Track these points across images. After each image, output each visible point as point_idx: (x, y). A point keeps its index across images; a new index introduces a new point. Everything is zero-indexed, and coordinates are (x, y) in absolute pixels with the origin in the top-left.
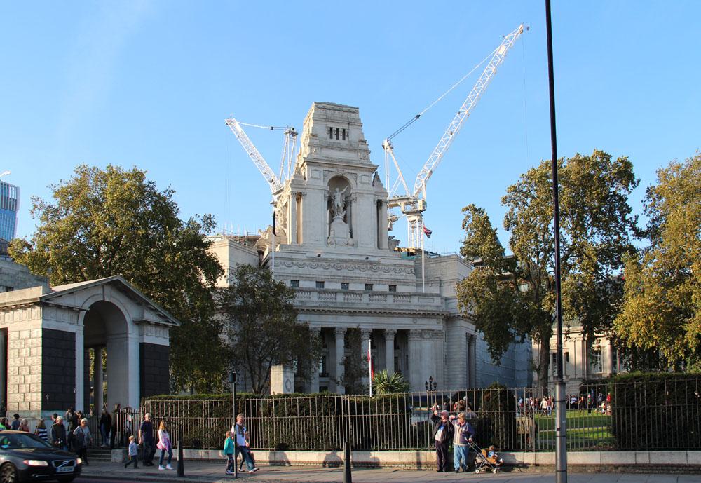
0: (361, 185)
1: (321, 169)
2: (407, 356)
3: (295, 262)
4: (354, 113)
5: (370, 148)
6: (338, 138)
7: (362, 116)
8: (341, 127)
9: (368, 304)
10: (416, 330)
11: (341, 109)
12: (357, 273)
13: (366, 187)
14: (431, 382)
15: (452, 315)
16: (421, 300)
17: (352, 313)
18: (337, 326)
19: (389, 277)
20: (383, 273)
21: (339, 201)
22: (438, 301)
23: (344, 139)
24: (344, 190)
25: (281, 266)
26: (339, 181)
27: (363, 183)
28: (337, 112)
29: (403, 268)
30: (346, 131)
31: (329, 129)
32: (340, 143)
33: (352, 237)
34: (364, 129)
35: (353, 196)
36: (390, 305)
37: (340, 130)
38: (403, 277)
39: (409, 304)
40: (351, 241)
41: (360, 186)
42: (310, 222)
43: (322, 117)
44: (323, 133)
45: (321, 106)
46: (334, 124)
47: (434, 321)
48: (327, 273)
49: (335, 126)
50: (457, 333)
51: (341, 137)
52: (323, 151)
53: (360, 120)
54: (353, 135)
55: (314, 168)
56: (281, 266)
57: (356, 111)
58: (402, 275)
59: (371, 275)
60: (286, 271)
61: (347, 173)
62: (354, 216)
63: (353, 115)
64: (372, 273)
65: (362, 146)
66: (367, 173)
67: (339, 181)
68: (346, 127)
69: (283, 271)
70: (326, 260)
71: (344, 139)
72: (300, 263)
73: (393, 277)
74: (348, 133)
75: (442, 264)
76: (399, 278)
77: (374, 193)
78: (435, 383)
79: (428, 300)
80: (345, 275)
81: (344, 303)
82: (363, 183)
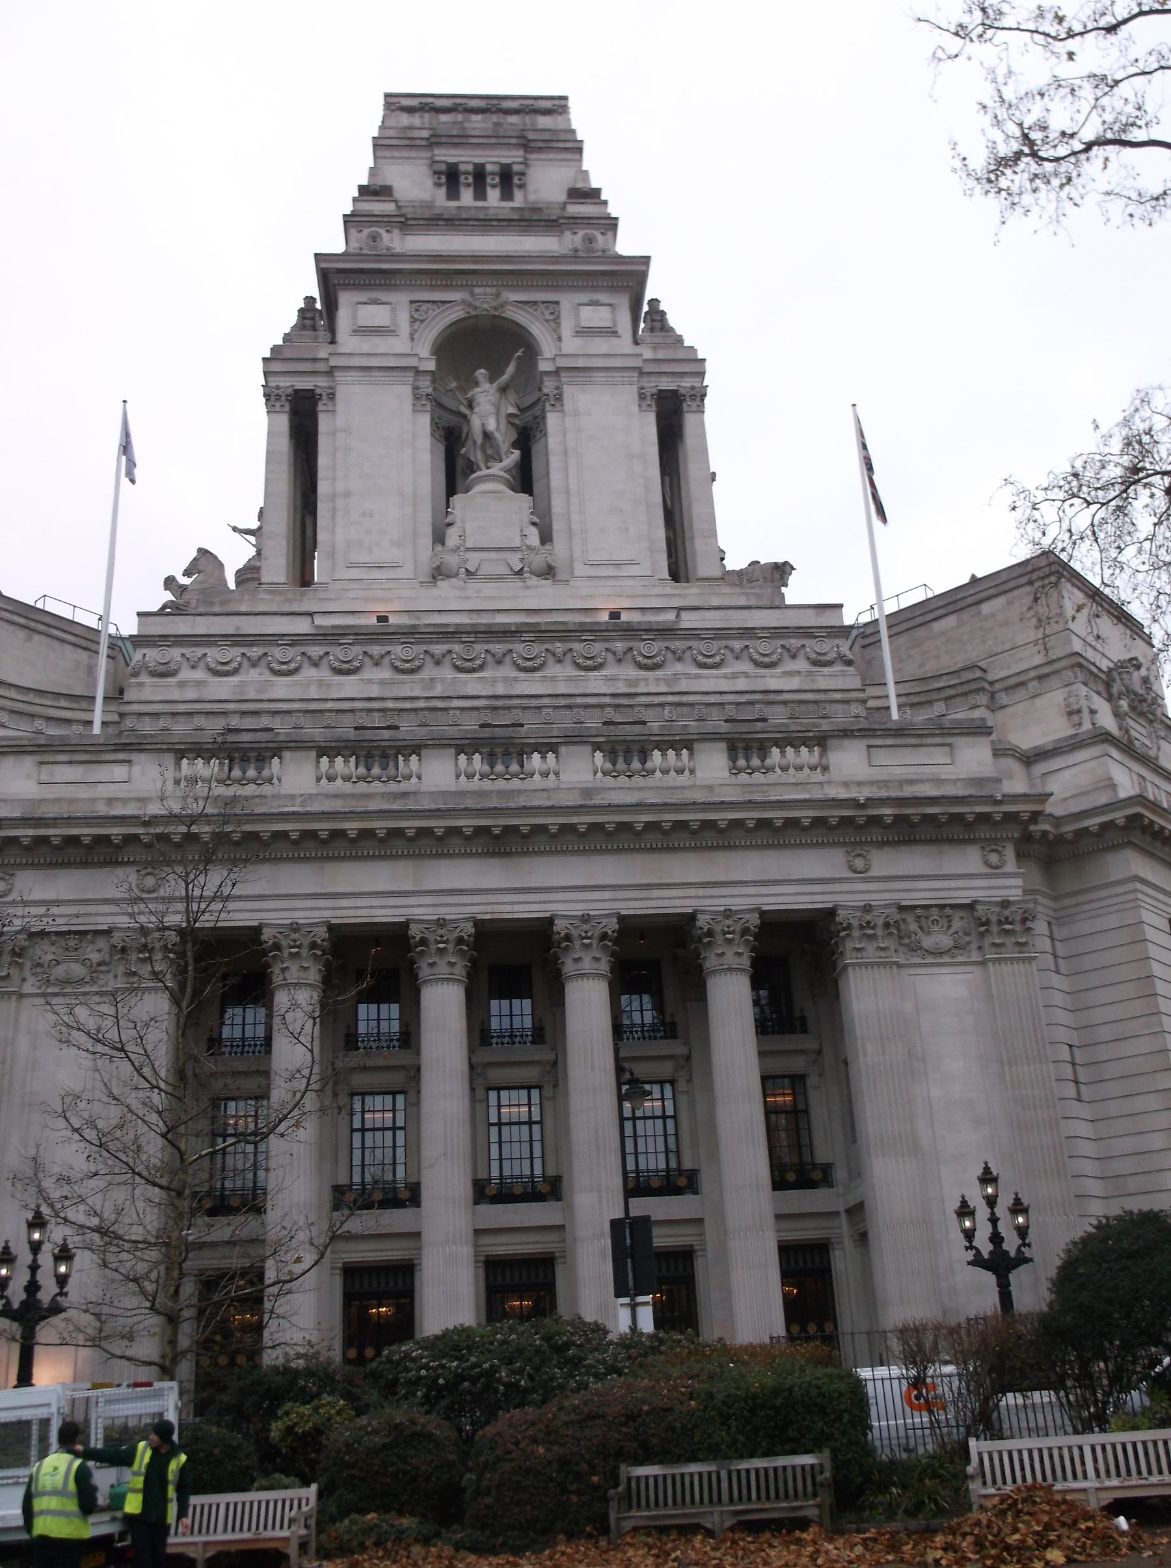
0: (579, 341)
1: (402, 299)
2: (846, 1063)
3: (255, 652)
4: (547, 112)
5: (613, 210)
6: (480, 194)
7: (582, 121)
8: (492, 159)
9: (587, 792)
10: (868, 908)
11: (492, 105)
12: (560, 678)
13: (600, 345)
14: (991, 1201)
15: (1068, 828)
16: (881, 757)
17: (503, 839)
18: (420, 911)
19: (724, 685)
20: (696, 671)
21: (488, 411)
22: (972, 760)
23: (507, 195)
25: (186, 674)
26: (483, 346)
27: (583, 332)
28: (479, 117)
29: (794, 643)
30: (516, 168)
31: (443, 167)
32: (487, 208)
33: (546, 537)
34: (589, 161)
35: (549, 385)
36: (710, 788)
37: (489, 168)
38: (794, 683)
39: (817, 776)
40: (538, 561)
41: (571, 344)
42: (347, 494)
43: (416, 134)
44: (414, 183)
45: (414, 102)
47: (970, 859)
48: (411, 687)
49: (466, 158)
50: (1113, 921)
51: (493, 195)
52: (408, 238)
53: (573, 132)
54: (546, 183)
55: (364, 296)
56: (186, 674)
57: (557, 106)
58: (790, 674)
59: (630, 682)
61: (515, 304)
62: (555, 462)
63: (543, 122)
64: (632, 672)
65: (574, 209)
66: (604, 297)
67: (483, 346)
68: (511, 156)
69: (190, 694)
70: (410, 634)
71: (507, 195)
72: (277, 653)
73: (742, 684)
74: (523, 174)
75: (986, 608)
76: (773, 684)
77: (637, 363)
78: (1018, 1207)
80: (501, 690)
81: (462, 794)
82: (583, 332)
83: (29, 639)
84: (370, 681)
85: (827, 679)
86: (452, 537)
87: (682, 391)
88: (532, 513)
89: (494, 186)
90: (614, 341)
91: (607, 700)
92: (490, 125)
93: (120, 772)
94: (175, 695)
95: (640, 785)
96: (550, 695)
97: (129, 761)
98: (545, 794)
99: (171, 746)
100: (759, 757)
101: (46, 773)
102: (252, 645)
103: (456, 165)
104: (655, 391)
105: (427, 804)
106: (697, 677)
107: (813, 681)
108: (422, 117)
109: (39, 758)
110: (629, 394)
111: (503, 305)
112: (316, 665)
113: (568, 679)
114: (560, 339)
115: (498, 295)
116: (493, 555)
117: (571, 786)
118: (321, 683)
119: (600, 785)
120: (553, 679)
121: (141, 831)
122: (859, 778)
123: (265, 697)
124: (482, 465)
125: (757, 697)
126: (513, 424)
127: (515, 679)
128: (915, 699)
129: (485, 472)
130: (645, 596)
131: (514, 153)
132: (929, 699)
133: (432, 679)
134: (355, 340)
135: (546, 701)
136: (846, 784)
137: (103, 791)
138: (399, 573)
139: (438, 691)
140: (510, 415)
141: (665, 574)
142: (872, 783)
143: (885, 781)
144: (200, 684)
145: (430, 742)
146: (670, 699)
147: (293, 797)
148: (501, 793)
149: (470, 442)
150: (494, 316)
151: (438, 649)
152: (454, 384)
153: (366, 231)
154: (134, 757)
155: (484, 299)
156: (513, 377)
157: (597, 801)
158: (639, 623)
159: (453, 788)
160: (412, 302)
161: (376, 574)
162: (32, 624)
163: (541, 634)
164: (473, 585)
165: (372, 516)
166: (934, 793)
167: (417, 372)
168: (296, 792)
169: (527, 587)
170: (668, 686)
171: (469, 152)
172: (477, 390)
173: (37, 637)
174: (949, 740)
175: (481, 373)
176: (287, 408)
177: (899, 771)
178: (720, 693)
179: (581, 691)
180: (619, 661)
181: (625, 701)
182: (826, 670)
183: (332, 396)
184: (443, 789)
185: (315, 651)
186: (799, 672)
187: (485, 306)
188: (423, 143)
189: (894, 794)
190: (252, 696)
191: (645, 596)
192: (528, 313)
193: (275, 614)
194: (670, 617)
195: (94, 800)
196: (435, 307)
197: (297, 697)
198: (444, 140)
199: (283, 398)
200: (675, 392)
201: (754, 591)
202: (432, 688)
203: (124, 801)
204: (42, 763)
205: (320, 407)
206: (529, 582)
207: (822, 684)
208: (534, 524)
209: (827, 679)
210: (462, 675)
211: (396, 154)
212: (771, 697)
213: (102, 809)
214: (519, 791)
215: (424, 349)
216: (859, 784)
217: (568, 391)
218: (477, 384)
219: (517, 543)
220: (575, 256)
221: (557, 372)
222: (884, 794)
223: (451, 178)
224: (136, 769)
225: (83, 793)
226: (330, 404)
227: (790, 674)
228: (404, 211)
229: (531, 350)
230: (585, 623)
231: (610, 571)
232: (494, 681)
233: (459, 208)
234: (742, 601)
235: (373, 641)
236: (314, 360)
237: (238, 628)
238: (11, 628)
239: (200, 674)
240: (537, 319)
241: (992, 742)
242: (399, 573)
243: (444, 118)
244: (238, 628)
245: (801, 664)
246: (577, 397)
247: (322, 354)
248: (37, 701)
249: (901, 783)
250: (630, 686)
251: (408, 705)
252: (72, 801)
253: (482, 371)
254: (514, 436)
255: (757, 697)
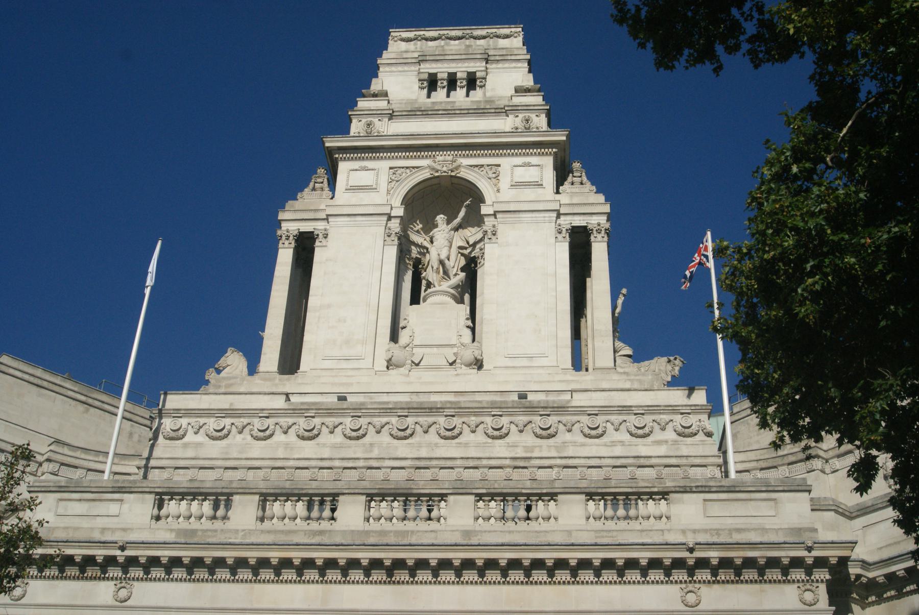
1: (383, 165)
8: (461, 70)
9: (467, 533)
13: (530, 194)
16: (716, 509)
19: (604, 452)
24: (462, 214)
28: (457, 42)
29: (665, 417)
30: (478, 75)
31: (426, 76)
32: (455, 102)
36: (569, 532)
37: (459, 75)
38: (662, 450)
43: (409, 55)
46: (439, 65)
49: (442, 70)
56: (190, 437)
60: (203, 453)
61: (467, 167)
66: (534, 160)
68: (477, 67)
69: (190, 453)
73: (618, 451)
74: (485, 79)
79: (750, 509)
80: (424, 453)
81: (367, 533)
83: (87, 411)
84: (324, 445)
85: (688, 447)
86: (404, 337)
87: (590, 227)
88: (467, 319)
89: (462, 87)
90: (540, 191)
91: (508, 462)
92: (463, 47)
93: (114, 508)
94: (179, 453)
95: (511, 529)
96: (462, 458)
97: (122, 500)
98: (433, 535)
99: (152, 490)
100: (625, 509)
101: (62, 508)
102: (240, 417)
103: (436, 74)
104: (569, 227)
105: (338, 540)
106: (583, 445)
107: (678, 449)
108: (415, 44)
109: (59, 495)
110: (549, 229)
111: (458, 167)
112: (286, 433)
113: (478, 445)
114: (498, 191)
115: (453, 161)
116: (435, 350)
117: (454, 528)
118: (287, 446)
119: (478, 528)
120: (466, 445)
121: (118, 553)
122: (697, 527)
123: (244, 456)
124: (436, 284)
125: (630, 461)
126: (462, 255)
127: (436, 445)
128: (764, 465)
129: (437, 288)
130: (549, 382)
131: (478, 64)
132: (775, 464)
133: (371, 444)
134: (348, 195)
135: (459, 462)
136: (684, 532)
137: (100, 522)
138: (361, 364)
139: (375, 453)
140: (460, 248)
141: (569, 364)
142: (705, 531)
143: (718, 530)
144: (199, 445)
145: (347, 491)
146: (559, 462)
147: (237, 531)
148: (398, 533)
149: (430, 268)
150: (451, 176)
151: (379, 421)
152: (421, 226)
153: (364, 121)
154: (126, 496)
155: (441, 163)
156: (463, 219)
157: (475, 541)
158: (539, 402)
159: (361, 529)
160: (391, 168)
161: (344, 365)
162: (90, 401)
163: (458, 410)
164: (416, 373)
165: (345, 322)
166: (758, 539)
167: (390, 218)
168: (240, 528)
169: (457, 375)
170: (558, 452)
171: (446, 65)
172: (435, 230)
173: (92, 410)
174: (774, 495)
175: (440, 218)
176: (293, 245)
177: (730, 521)
178: (600, 458)
179: (487, 455)
180: (521, 431)
181: (522, 464)
182: (689, 440)
183: (326, 236)
184: (353, 528)
185: (284, 421)
186: (666, 442)
187: (445, 169)
188: (414, 61)
189: (722, 539)
190: (235, 455)
191: (549, 382)
192: (475, 172)
193: (260, 393)
194: (567, 397)
195: (92, 529)
196: (408, 171)
197: (267, 457)
198: (428, 58)
199: (291, 238)
200: (585, 228)
201: (637, 378)
202: (371, 451)
203: (113, 530)
204: (61, 500)
205: (317, 243)
206: (459, 371)
207: (685, 451)
208: (468, 327)
209: (688, 447)
210: (396, 441)
211: (393, 69)
212: (642, 461)
213: (97, 536)
214: (412, 532)
215: (397, 201)
216: (694, 531)
217: (501, 229)
218: (436, 226)
219: (454, 341)
220: (515, 131)
221: (495, 215)
222: (715, 539)
223: (432, 83)
224: (125, 507)
225: (85, 523)
226: (324, 240)
227: (659, 443)
228: (393, 107)
229: (478, 198)
230: (495, 402)
231: (525, 362)
232: (420, 446)
233: (433, 103)
234: (627, 385)
235: (330, 415)
236: (316, 210)
237: (231, 404)
238: (74, 403)
239: (201, 438)
240: (483, 177)
241: (812, 499)
242: (361, 364)
243: (430, 43)
244: (231, 404)
245: (670, 435)
246: (507, 231)
247: (322, 207)
248: (83, 456)
249: (730, 531)
250: (526, 452)
251: (350, 464)
252: (76, 529)
253: (442, 216)
254: (463, 262)
255: (630, 461)
